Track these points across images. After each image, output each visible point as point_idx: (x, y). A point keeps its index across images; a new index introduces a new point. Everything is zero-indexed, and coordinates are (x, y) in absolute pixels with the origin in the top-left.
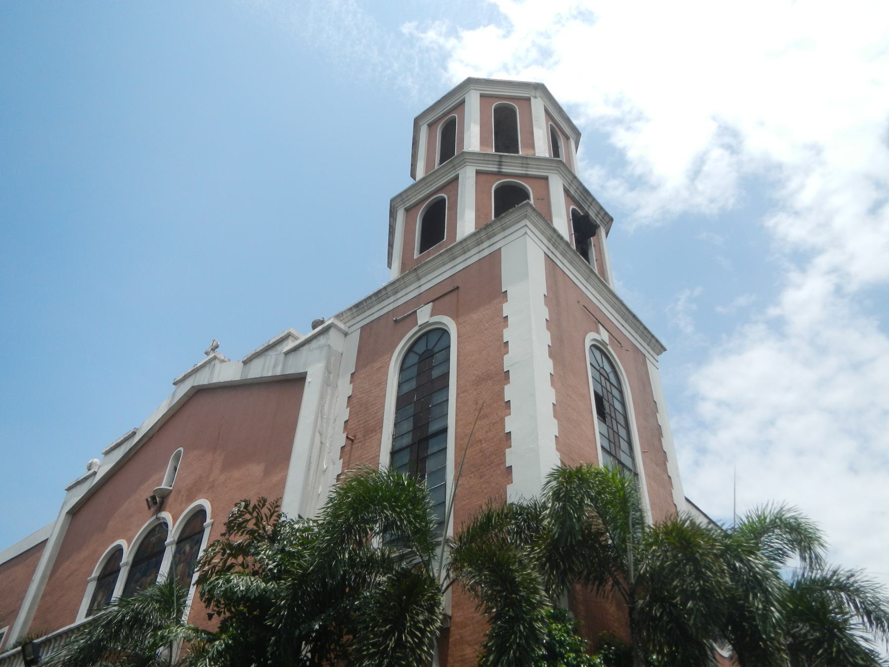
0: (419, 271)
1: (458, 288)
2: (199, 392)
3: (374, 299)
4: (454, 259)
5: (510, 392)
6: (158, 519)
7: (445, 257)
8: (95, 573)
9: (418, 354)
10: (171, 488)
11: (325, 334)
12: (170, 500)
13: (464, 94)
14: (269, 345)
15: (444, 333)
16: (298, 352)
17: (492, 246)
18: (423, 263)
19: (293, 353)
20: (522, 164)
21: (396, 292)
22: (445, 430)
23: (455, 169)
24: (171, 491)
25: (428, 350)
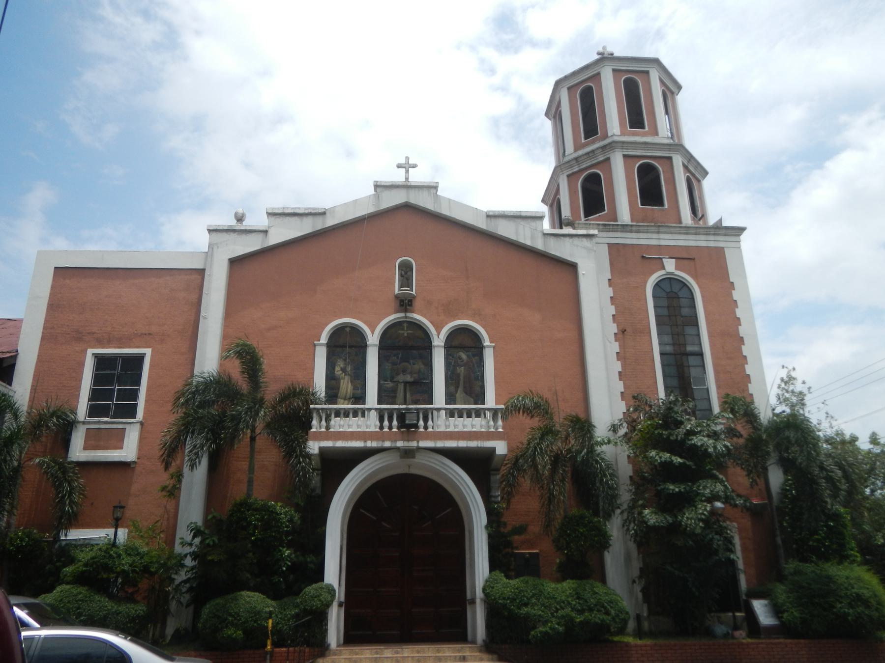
1: (694, 259)
2: (407, 207)
3: (619, 227)
4: (687, 234)
5: (746, 350)
6: (406, 317)
7: (683, 230)
8: (324, 339)
9: (666, 292)
10: (414, 293)
11: (588, 239)
12: (417, 304)
13: (650, 68)
14: (520, 216)
15: (683, 287)
16: (558, 239)
17: (716, 242)
18: (666, 225)
19: (553, 237)
21: (638, 232)
22: (701, 354)
23: (669, 151)
24: (414, 297)
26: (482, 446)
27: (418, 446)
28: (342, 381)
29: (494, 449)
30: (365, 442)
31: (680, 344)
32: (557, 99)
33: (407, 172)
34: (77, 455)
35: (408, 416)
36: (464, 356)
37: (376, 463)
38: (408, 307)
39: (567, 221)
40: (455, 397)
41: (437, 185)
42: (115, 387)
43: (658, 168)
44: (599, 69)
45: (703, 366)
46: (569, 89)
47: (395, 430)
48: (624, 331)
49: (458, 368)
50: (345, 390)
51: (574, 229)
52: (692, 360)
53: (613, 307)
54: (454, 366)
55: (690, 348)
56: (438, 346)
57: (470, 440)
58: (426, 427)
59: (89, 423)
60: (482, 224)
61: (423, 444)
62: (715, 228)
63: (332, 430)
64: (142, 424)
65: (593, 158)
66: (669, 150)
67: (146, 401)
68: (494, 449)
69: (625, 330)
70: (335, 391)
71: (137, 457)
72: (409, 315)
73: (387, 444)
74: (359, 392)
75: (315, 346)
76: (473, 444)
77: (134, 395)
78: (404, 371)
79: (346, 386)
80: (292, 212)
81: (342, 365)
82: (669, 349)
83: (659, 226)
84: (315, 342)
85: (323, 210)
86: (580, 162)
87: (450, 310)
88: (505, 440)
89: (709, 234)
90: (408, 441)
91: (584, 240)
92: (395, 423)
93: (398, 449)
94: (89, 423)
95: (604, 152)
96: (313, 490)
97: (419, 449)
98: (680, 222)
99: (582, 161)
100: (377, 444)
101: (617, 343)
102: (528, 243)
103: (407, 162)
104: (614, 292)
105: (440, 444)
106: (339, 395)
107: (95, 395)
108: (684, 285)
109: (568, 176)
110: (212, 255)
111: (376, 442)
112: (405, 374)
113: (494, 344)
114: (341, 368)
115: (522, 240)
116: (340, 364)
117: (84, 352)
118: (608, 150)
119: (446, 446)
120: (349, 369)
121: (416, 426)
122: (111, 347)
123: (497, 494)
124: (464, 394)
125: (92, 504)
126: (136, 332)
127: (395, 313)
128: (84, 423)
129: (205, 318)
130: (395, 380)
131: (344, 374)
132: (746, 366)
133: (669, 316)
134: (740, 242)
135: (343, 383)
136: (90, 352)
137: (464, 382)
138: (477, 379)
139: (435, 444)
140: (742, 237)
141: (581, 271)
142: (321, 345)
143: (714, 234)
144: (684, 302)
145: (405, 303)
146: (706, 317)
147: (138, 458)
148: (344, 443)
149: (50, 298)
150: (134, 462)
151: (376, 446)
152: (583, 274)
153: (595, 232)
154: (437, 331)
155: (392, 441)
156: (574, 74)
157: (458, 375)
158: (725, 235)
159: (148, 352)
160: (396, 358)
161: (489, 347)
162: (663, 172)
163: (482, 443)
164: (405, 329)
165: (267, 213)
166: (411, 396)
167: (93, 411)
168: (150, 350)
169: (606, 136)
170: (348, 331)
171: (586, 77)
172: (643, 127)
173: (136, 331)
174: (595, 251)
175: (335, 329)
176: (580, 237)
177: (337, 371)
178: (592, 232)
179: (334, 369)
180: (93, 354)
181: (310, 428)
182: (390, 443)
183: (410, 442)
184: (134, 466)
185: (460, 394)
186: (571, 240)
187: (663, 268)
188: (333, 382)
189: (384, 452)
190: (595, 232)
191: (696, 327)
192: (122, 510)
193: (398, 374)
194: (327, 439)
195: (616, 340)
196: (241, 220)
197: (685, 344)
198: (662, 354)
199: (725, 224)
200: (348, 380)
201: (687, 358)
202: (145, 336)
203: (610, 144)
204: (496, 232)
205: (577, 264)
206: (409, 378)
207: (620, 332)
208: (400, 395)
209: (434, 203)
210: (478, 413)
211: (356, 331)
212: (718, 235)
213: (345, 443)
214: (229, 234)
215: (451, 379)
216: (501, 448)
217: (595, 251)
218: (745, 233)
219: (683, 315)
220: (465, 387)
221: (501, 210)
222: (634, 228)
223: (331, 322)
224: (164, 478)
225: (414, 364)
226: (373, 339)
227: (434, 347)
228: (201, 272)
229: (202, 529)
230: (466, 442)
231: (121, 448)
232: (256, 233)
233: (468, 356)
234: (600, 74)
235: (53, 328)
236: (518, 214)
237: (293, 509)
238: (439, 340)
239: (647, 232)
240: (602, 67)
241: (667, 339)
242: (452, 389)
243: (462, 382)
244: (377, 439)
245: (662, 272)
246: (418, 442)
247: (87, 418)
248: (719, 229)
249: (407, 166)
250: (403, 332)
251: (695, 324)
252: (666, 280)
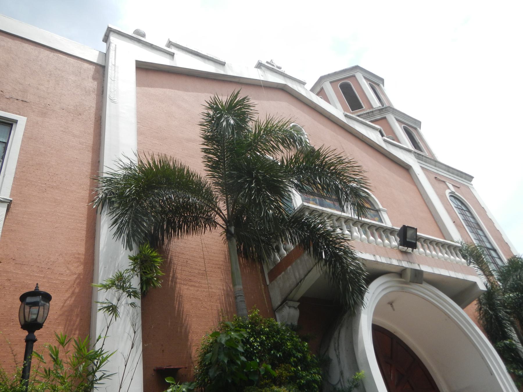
0: (437, 164)
65: (372, 117)
156: (336, 74)
189: (387, 275)
202: (16, 101)
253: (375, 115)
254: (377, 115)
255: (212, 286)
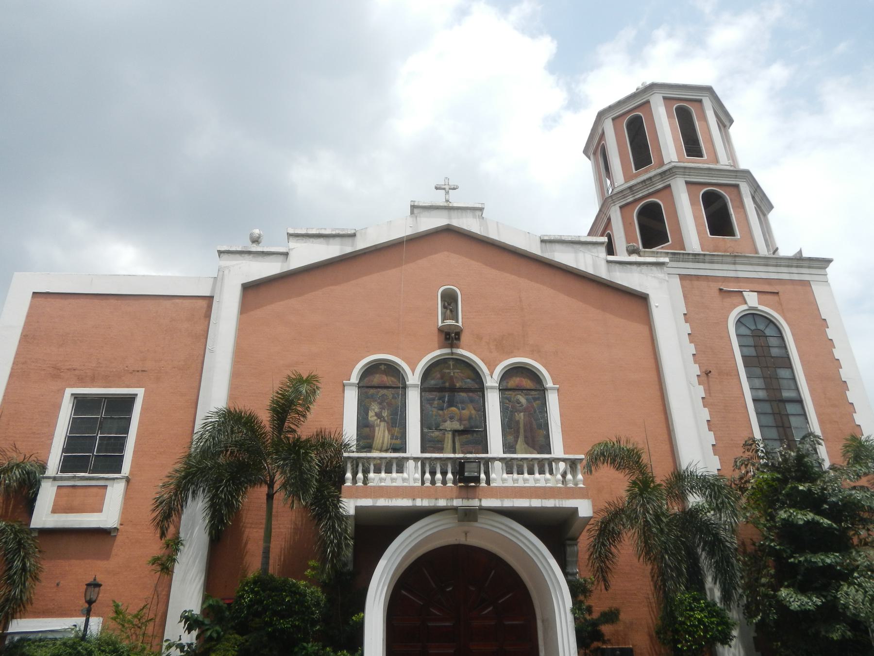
0: (737, 259)
1: (778, 293)
2: (449, 230)
4: (767, 265)
6: (452, 354)
8: (354, 378)
9: (751, 330)
11: (658, 268)
12: (464, 338)
18: (743, 254)
19: (618, 265)
20: (761, 198)
22: (800, 401)
23: (736, 178)
25: (757, 329)
26: (561, 506)
27: (480, 506)
28: (377, 429)
29: (575, 510)
30: (414, 499)
31: (774, 389)
32: (600, 131)
33: (447, 193)
34: (44, 519)
35: (467, 466)
36: (523, 400)
37: (432, 526)
38: (455, 342)
39: (633, 248)
40: (515, 449)
41: (483, 206)
42: (97, 435)
43: (725, 196)
44: (649, 96)
45: (804, 415)
46: (613, 119)
47: (450, 484)
48: (708, 373)
49: (516, 413)
50: (381, 439)
51: (640, 256)
52: (791, 408)
53: (693, 345)
54: (511, 412)
55: (786, 394)
56: (492, 388)
57: (545, 499)
58: (488, 482)
59: (61, 479)
60: (535, 249)
61: (487, 503)
62: (798, 259)
63: (370, 484)
64: (128, 480)
65: (650, 186)
66: (736, 177)
67: (135, 452)
68: (575, 510)
69: (710, 372)
70: (368, 441)
71: (119, 523)
72: (455, 351)
73: (442, 503)
74: (398, 442)
75: (344, 386)
76: (550, 503)
77: (120, 445)
78: (452, 418)
79: (382, 434)
80: (318, 233)
81: (377, 410)
82: (762, 394)
83: (735, 256)
84: (344, 382)
85: (353, 232)
86: (635, 191)
87: (503, 346)
88: (588, 498)
89: (792, 266)
90: (468, 498)
91: (654, 268)
92: (450, 476)
93: (455, 509)
94: (61, 479)
95: (664, 178)
96: (345, 564)
97: (482, 509)
98: (757, 252)
99: (637, 190)
100: (429, 503)
101: (701, 387)
102: (590, 270)
103: (447, 183)
104: (692, 328)
105: (508, 503)
106: (374, 446)
107: (71, 444)
108: (770, 322)
109: (621, 207)
110: (222, 279)
111: (427, 500)
112: (453, 421)
113: (558, 386)
114: (375, 413)
115: (582, 267)
116: (375, 408)
117: (62, 392)
118: (668, 177)
119: (515, 506)
120: (385, 414)
121: (477, 480)
122: (94, 387)
123: (575, 571)
124: (526, 446)
125: (58, 585)
126: (126, 368)
127: (440, 348)
128: (55, 479)
129: (212, 351)
130: (441, 428)
131: (379, 420)
132: (854, 414)
133: (758, 357)
134: (826, 275)
135: (379, 429)
136: (69, 391)
137: (525, 431)
138: (540, 427)
139: (502, 504)
140: (827, 270)
141: (654, 302)
142: (352, 385)
143: (797, 267)
144: (773, 342)
145: (451, 337)
146: (801, 358)
147: (121, 524)
148: (387, 501)
149: (24, 328)
150: (116, 529)
151: (427, 505)
152: (657, 307)
153: (666, 260)
154: (489, 369)
155: (448, 499)
156: (620, 103)
157: (518, 422)
158: (809, 267)
159: (140, 392)
160: (441, 401)
161: (552, 389)
162: (731, 200)
163: (561, 502)
164: (452, 368)
165: (288, 233)
166: (461, 448)
167: (69, 464)
168: (143, 390)
169: (662, 163)
170: (383, 369)
171: (634, 105)
172: (701, 156)
173: (127, 367)
174: (668, 281)
175: (365, 368)
176: (649, 266)
177: (371, 417)
178: (662, 260)
179: (367, 414)
180: (72, 394)
181: (343, 481)
182: (445, 501)
183: (470, 500)
184: (115, 534)
185: (520, 444)
186: (639, 269)
187: (746, 303)
188: (367, 429)
189: (436, 514)
190: (666, 260)
191: (790, 370)
192: (97, 589)
193: (445, 421)
194: (366, 497)
195: (700, 384)
196: (257, 241)
197: (780, 389)
198: (755, 400)
199: (805, 255)
200: (385, 427)
201: (785, 405)
202: (137, 374)
203: (670, 169)
204: (553, 259)
205: (648, 295)
206: (457, 426)
207: (704, 374)
208: (448, 443)
209: (480, 226)
210: (545, 466)
211: (391, 369)
212: (802, 267)
213: (387, 501)
214: (244, 257)
215: (509, 427)
216: (585, 508)
217: (668, 281)
218: (831, 264)
219: (773, 355)
220: (526, 437)
221: (557, 234)
222: (707, 258)
223: (363, 358)
224: (156, 548)
225: (463, 409)
226: (414, 378)
227: (487, 389)
228: (210, 299)
229: (201, 619)
230: (540, 500)
231: (100, 510)
232: (275, 255)
233: (527, 400)
234: (649, 102)
235: (25, 363)
236: (577, 239)
237: (319, 589)
238: (492, 380)
239: (722, 263)
240: (652, 95)
241: (759, 383)
242: (511, 438)
243: (522, 431)
244: (429, 497)
245: (745, 307)
246: (480, 500)
247: (59, 473)
248: (799, 261)
249: (447, 187)
250: (447, 371)
251: (790, 366)
252: (749, 316)
253: (654, 182)
254: (659, 182)
255: (281, 526)
